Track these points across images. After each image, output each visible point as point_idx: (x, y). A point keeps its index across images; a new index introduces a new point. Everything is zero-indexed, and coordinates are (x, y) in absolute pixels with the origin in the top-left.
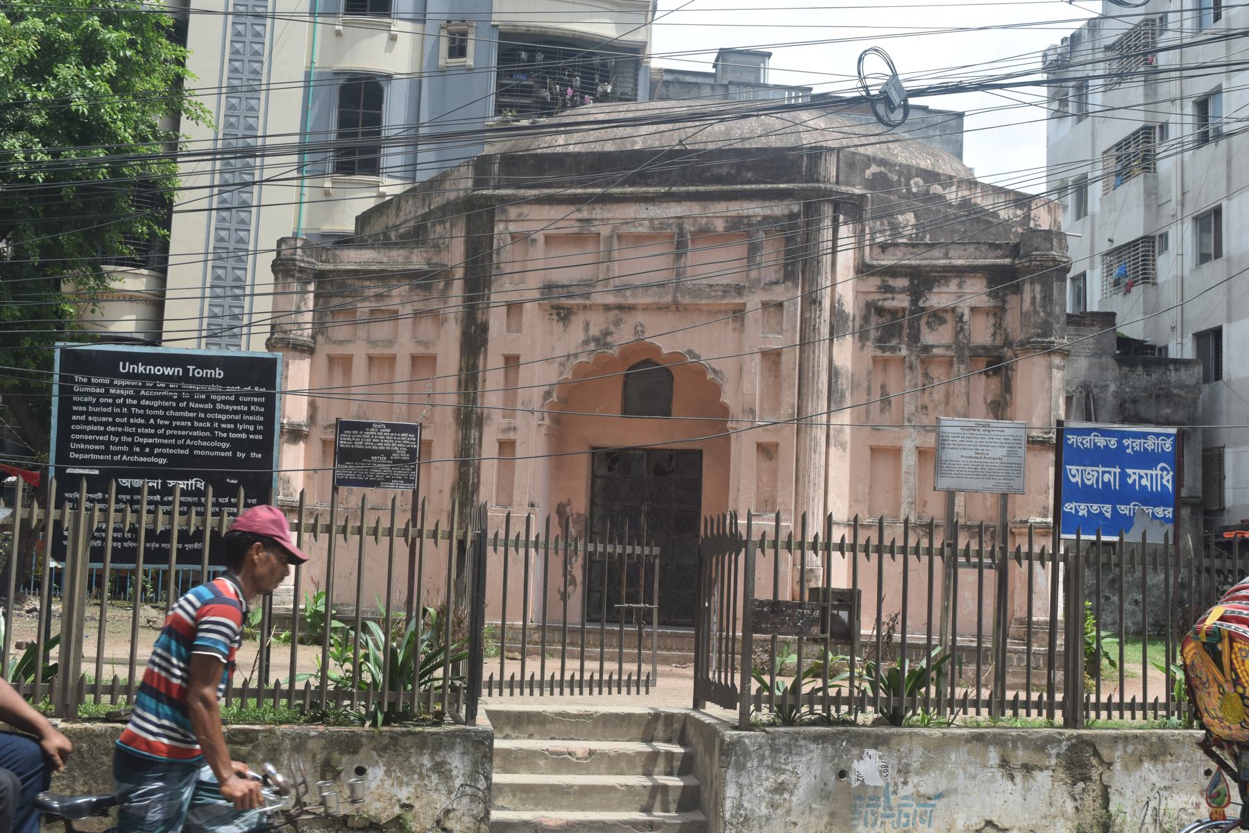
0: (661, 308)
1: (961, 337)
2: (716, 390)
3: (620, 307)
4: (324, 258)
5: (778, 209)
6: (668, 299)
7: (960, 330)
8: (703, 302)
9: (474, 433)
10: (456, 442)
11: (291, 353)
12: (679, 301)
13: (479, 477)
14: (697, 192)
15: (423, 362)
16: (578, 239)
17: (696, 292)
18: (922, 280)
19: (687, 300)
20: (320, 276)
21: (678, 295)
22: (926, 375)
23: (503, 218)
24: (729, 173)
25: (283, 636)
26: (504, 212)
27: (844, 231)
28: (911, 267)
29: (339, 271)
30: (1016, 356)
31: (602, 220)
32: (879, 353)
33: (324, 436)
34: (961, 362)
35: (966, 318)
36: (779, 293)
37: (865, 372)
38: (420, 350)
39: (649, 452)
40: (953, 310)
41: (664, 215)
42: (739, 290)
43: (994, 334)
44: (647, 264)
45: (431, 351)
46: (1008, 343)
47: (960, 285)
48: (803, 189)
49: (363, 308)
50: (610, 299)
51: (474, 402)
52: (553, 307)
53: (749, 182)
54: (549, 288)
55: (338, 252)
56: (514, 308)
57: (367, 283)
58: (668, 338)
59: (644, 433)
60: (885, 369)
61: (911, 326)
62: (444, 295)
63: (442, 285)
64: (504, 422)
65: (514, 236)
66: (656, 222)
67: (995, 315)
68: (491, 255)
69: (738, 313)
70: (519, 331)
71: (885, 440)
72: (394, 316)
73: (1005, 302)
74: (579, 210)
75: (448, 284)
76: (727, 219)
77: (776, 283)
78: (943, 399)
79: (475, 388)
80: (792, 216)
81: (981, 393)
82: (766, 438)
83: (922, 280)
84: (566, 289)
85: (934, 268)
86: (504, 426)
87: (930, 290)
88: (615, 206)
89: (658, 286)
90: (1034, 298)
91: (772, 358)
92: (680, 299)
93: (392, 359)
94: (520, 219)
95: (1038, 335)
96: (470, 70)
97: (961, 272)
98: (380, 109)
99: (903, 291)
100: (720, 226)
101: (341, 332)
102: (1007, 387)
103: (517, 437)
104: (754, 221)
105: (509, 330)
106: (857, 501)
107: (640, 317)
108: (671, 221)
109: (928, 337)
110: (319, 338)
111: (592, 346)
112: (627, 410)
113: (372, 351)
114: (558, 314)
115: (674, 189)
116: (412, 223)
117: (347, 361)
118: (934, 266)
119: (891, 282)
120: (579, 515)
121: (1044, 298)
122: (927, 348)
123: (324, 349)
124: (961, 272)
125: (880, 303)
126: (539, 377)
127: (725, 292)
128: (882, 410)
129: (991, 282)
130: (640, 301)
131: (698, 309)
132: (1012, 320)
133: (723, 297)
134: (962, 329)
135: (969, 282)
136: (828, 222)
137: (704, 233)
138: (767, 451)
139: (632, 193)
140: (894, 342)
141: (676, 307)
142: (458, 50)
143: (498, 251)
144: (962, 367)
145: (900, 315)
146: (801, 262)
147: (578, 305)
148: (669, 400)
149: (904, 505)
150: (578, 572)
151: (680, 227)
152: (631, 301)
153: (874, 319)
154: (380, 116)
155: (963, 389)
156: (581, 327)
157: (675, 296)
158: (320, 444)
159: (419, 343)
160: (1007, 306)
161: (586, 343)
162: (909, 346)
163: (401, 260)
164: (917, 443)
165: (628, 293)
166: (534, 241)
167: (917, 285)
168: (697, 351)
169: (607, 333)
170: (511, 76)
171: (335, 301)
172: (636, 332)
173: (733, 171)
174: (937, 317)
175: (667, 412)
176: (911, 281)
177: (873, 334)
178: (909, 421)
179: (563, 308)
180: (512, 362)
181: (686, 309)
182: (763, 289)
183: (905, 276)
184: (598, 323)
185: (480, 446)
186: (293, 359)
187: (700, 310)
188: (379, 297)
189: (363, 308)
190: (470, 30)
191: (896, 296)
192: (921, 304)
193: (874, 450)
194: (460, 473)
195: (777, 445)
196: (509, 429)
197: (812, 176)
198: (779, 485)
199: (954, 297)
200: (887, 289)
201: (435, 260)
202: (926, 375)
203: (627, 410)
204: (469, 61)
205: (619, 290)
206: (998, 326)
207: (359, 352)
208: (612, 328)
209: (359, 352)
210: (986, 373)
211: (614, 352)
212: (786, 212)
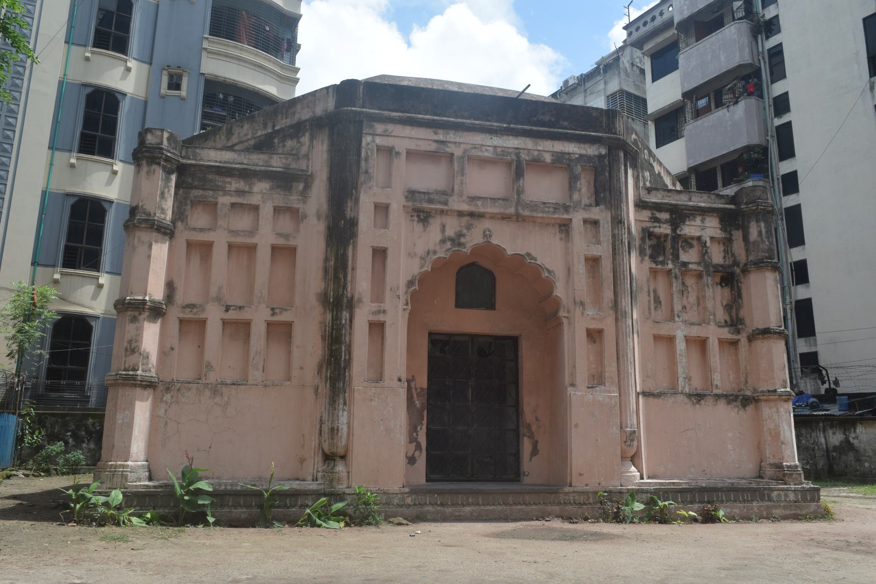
0: (504, 218)
1: (706, 257)
2: (549, 286)
3: (472, 215)
4: (184, 153)
5: (591, 150)
6: (512, 210)
7: (704, 252)
8: (540, 215)
9: (345, 315)
10: (323, 323)
11: (155, 234)
12: (520, 215)
13: (350, 354)
14: (531, 130)
15: (284, 253)
16: (432, 156)
17: (533, 206)
18: (679, 215)
19: (526, 213)
20: (182, 170)
21: (520, 208)
22: (683, 283)
23: (371, 131)
24: (550, 121)
25: (149, 516)
26: (372, 127)
27: (630, 172)
28: (671, 205)
29: (202, 165)
30: (745, 271)
31: (455, 143)
32: (654, 266)
33: (181, 315)
34: (708, 275)
35: (708, 244)
36: (596, 213)
37: (645, 279)
38: (281, 242)
39: (473, 337)
40: (699, 238)
41: (505, 145)
42: (566, 209)
43: (724, 257)
44: (488, 183)
45: (292, 242)
46: (736, 263)
47: (703, 221)
48: (609, 138)
49: (224, 200)
50: (465, 207)
51: (345, 287)
52: (414, 210)
53: (565, 128)
54: (412, 194)
55: (197, 150)
56: (382, 209)
57: (229, 180)
58: (510, 240)
59: (475, 322)
60: (655, 278)
61: (673, 247)
62: (304, 195)
63: (301, 186)
64: (375, 306)
65: (379, 149)
66: (499, 150)
67: (724, 244)
68: (358, 162)
69: (565, 227)
70: (385, 226)
71: (665, 330)
72: (255, 208)
73: (731, 235)
74: (436, 133)
75: (307, 187)
76: (553, 153)
77: (590, 206)
78: (696, 302)
79: (345, 276)
80: (600, 157)
81: (718, 299)
82: (594, 326)
83: (679, 215)
84: (428, 195)
85: (687, 208)
86: (374, 309)
87: (684, 222)
88: (465, 134)
89: (504, 200)
90: (760, 233)
91: (593, 262)
92: (521, 211)
93: (252, 249)
94: (385, 134)
95: (766, 258)
96: (183, 99)
97: (703, 212)
98: (117, 114)
99: (666, 222)
100: (548, 158)
101: (199, 218)
102: (740, 296)
103: (388, 319)
104: (573, 157)
105: (375, 226)
106: (648, 376)
107: (487, 224)
108: (510, 150)
109: (684, 257)
110: (179, 224)
111: (448, 245)
112: (459, 304)
113: (233, 240)
114: (418, 216)
115: (512, 126)
116: (252, 142)
117: (206, 248)
118: (686, 205)
119: (658, 215)
120: (422, 389)
121: (767, 232)
122: (685, 264)
123: (183, 236)
124: (703, 212)
125: (651, 229)
126: (403, 269)
127: (555, 209)
128: (656, 308)
129: (722, 220)
130: (489, 210)
131: (533, 220)
132: (738, 247)
133: (554, 213)
134: (706, 252)
135: (708, 219)
136: (623, 167)
137: (537, 163)
138: (594, 336)
139: (480, 124)
140: (661, 259)
141: (518, 218)
142: (175, 85)
143: (367, 159)
144: (709, 279)
145: (662, 239)
146: (607, 193)
147: (436, 210)
148: (493, 296)
149: (680, 380)
150: (423, 440)
151: (518, 155)
152: (482, 210)
153: (648, 243)
154: (116, 119)
155: (711, 295)
156: (438, 228)
157: (517, 209)
158: (177, 322)
159: (279, 235)
160: (733, 238)
161: (443, 241)
162: (673, 262)
163: (261, 163)
164: (685, 333)
165: (479, 203)
166: (398, 154)
167: (675, 219)
168: (534, 254)
169: (460, 235)
170: (211, 107)
171: (195, 193)
172: (485, 236)
173: (553, 119)
174: (688, 242)
175: (491, 306)
176: (671, 215)
177: (648, 252)
178: (679, 317)
179: (423, 212)
180: (380, 254)
181: (524, 220)
182: (584, 209)
183: (667, 212)
184: (453, 226)
185: (351, 326)
186: (156, 242)
187: (534, 222)
188: (240, 193)
189: (224, 200)
190: (185, 74)
191: (662, 225)
192: (678, 232)
193: (657, 338)
194: (331, 351)
195: (600, 332)
196: (379, 312)
197: (611, 128)
198: (606, 363)
199: (699, 229)
200: (656, 220)
201: (293, 166)
202: (683, 283)
203: (459, 304)
204: (183, 93)
205: (473, 199)
206: (728, 251)
207: (220, 240)
208: (465, 231)
209: (220, 240)
210: (721, 284)
211: (467, 250)
212: (596, 153)
